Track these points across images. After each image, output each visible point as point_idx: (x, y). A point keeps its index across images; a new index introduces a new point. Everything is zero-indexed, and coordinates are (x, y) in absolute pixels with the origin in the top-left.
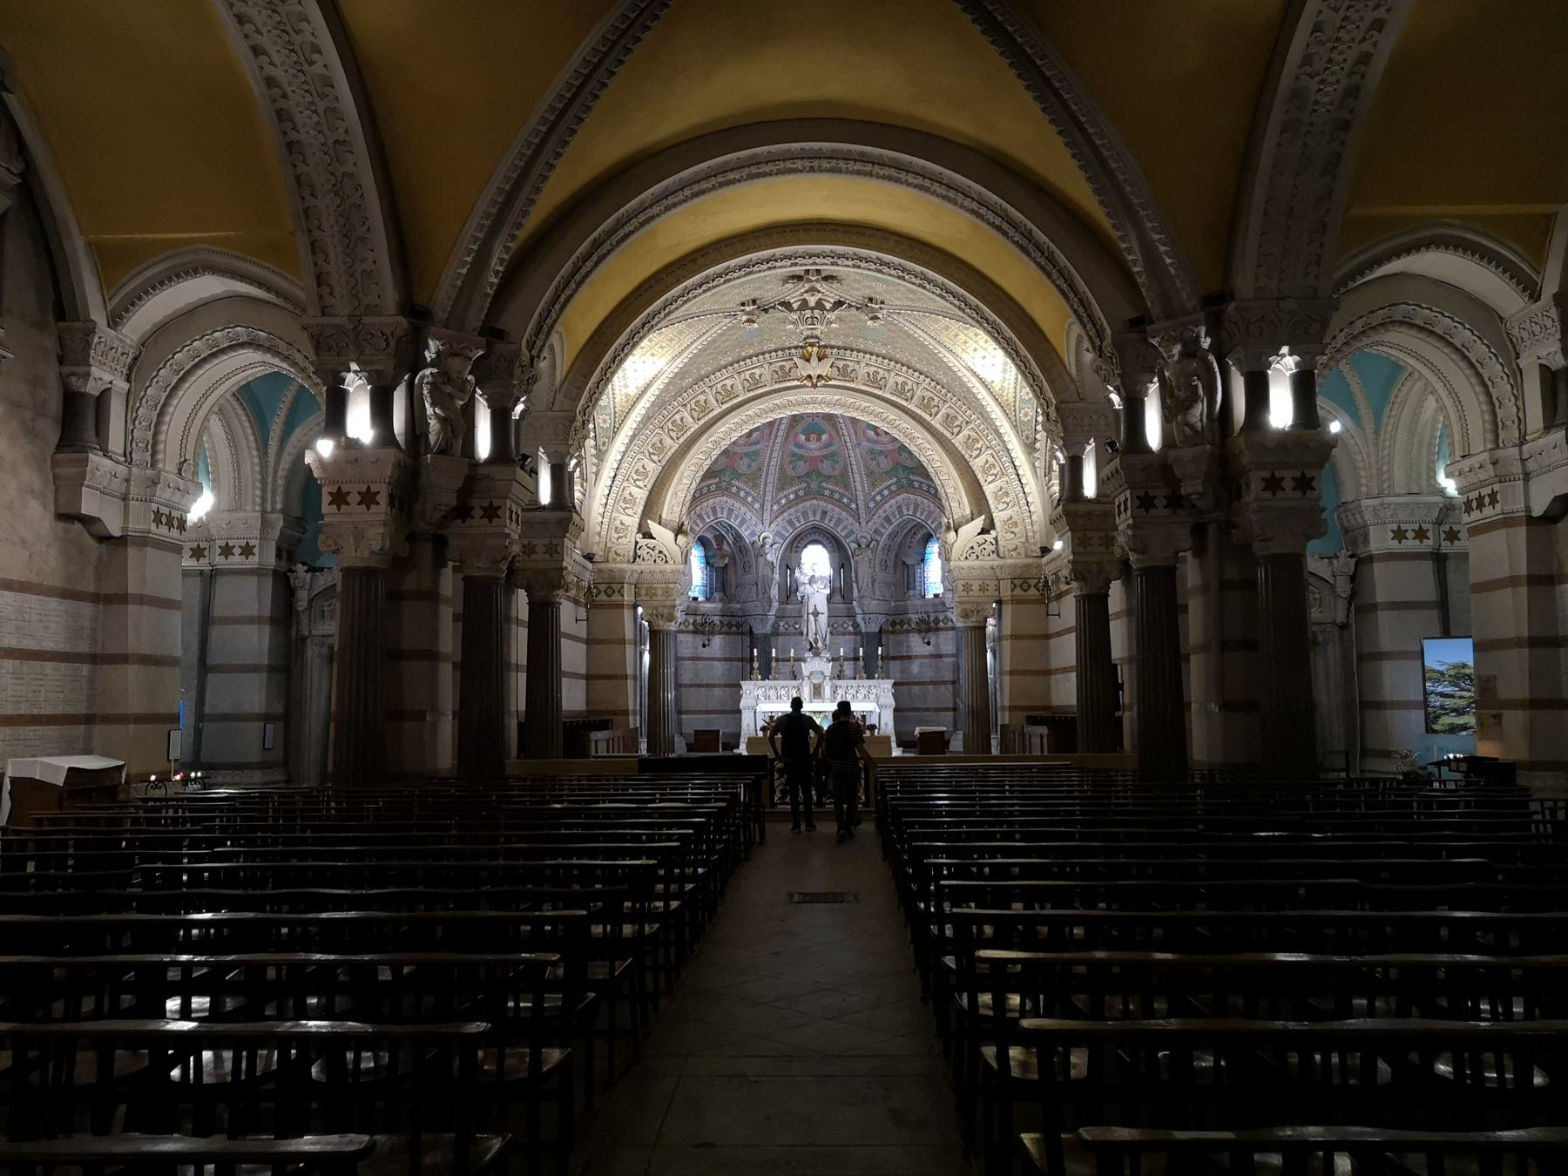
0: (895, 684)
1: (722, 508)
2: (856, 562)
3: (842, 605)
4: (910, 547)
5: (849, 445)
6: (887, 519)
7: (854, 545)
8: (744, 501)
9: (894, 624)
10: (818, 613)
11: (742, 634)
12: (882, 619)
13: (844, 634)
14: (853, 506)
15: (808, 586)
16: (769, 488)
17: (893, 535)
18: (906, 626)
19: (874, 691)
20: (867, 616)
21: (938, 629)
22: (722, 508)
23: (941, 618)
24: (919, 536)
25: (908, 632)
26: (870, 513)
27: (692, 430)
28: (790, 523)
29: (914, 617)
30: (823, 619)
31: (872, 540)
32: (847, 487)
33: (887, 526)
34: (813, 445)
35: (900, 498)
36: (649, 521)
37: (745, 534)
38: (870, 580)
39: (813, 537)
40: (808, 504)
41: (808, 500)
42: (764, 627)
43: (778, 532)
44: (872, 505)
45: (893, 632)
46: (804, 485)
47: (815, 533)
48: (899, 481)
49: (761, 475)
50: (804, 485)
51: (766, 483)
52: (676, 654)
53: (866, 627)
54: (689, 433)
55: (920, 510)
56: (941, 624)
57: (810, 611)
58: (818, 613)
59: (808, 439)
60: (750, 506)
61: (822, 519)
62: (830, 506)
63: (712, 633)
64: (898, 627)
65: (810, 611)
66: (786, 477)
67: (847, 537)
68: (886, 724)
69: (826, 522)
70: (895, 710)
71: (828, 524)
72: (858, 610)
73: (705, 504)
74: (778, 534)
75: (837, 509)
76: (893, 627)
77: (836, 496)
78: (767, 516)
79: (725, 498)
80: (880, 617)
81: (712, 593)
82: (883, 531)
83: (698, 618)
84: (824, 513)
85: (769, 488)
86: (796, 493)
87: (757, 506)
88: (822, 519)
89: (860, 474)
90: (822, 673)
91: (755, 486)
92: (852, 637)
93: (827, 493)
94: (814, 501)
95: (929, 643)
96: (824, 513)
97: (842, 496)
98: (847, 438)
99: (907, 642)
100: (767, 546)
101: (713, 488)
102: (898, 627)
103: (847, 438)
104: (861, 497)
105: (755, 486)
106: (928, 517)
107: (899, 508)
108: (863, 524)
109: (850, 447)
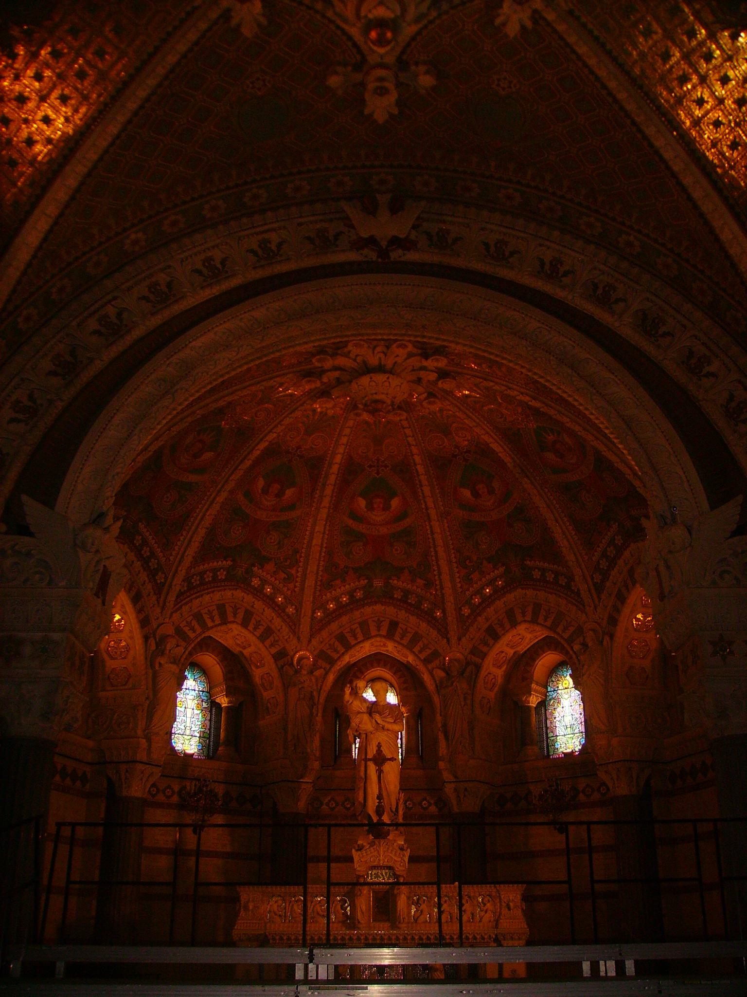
0: (525, 898)
5: (432, 512)
8: (270, 601)
15: (366, 717)
16: (310, 582)
27: (138, 333)
30: (392, 772)
34: (378, 517)
36: (25, 498)
40: (368, 610)
43: (322, 651)
44: (466, 611)
54: (129, 339)
56: (582, 797)
57: (370, 756)
59: (370, 507)
60: (280, 610)
62: (402, 614)
65: (370, 756)
72: (446, 776)
73: (207, 598)
75: (413, 619)
77: (412, 600)
78: (305, 627)
79: (239, 594)
81: (216, 750)
85: (310, 582)
87: (291, 610)
93: (398, 595)
94: (379, 607)
98: (430, 504)
100: (304, 672)
101: (222, 575)
103: (430, 504)
108: (454, 640)
109: (434, 516)
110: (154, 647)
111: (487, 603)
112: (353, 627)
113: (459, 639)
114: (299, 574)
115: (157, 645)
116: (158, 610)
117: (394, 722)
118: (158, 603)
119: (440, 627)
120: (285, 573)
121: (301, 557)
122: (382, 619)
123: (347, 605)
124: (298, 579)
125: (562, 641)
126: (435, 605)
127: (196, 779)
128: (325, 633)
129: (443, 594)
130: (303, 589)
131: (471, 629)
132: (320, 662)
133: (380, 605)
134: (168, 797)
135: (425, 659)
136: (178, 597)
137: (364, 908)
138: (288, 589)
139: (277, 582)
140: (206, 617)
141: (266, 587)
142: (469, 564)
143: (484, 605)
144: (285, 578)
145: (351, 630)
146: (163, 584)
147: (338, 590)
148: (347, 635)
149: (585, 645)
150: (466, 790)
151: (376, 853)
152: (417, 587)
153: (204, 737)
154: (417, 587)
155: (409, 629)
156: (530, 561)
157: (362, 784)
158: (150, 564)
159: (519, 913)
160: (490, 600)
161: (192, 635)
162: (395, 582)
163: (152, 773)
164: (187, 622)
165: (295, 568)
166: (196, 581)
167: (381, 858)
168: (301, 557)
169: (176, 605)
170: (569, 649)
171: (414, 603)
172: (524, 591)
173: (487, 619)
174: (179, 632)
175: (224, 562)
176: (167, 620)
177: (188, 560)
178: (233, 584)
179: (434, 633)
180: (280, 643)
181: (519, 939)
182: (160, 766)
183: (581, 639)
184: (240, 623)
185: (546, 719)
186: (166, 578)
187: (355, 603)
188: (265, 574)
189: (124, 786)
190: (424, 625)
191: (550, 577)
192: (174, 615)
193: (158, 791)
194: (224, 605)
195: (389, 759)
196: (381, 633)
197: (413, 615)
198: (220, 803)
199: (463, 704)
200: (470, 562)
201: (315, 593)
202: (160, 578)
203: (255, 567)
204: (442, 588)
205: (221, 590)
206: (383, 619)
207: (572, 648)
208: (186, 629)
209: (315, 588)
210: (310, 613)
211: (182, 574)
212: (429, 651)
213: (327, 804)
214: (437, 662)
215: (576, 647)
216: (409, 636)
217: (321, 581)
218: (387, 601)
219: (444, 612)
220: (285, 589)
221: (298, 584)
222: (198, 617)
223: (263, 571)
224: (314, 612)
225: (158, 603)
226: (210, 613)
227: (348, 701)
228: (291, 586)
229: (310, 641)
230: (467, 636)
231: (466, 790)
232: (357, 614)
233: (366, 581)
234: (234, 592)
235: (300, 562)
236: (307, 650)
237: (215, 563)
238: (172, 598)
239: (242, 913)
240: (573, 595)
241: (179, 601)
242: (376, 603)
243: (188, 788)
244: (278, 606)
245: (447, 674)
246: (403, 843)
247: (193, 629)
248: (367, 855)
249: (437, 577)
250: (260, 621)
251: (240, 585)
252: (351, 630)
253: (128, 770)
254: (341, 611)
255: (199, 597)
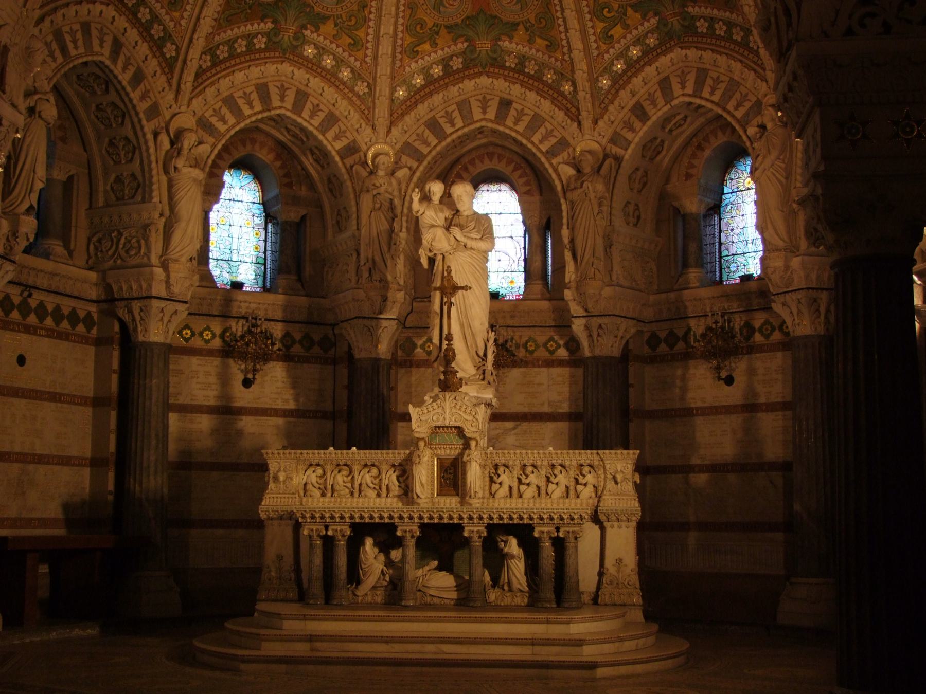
0: (641, 468)
1: (283, 90)
2: (572, 204)
3: (545, 305)
4: (688, 176)
6: (640, 112)
7: (568, 171)
8: (331, 77)
9: (654, 340)
10: (456, 288)
11: (334, 362)
12: (626, 329)
13: (549, 364)
14: (567, 88)
15: (440, 232)
16: (386, 47)
17: (651, 148)
18: (681, 346)
19: (590, 478)
20: (596, 322)
21: (751, 350)
22: (283, 90)
23: (757, 324)
24: (708, 153)
25: (687, 356)
26: (603, 103)
28: (433, 126)
29: (698, 327)
31: (606, 156)
32: (552, 46)
33: (637, 124)
35: (664, 60)
37: (333, 145)
38: (600, 242)
39: (487, 165)
41: (470, 77)
42: (376, 342)
43: (407, 145)
44: (605, 82)
45: (652, 360)
46: (462, 46)
47: (491, 156)
48: (663, 22)
49: (366, 20)
50: (462, 46)
51: (377, 38)
52: (166, 395)
53: (592, 345)
55: (709, 81)
56: (758, 338)
58: (456, 288)
61: (501, 116)
62: (516, 90)
63: (266, 358)
64: (663, 348)
66: (422, 24)
67: (551, 153)
68: (619, 561)
69: (510, 122)
70: (641, 527)
71: (514, 128)
72: (575, 309)
73: (239, 77)
74: (407, 149)
75: (532, 96)
76: (653, 347)
77: (531, 68)
78: (382, 112)
79: (286, 68)
80: (624, 324)
82: (629, 136)
83: (233, 323)
84: (505, 104)
85: (386, 47)
86: (445, 62)
87: (361, 88)
88: (501, 116)
89: (579, 13)
90: (460, 430)
91: (356, 45)
92: (565, 371)
93: (510, 62)
94: (484, 81)
95: (729, 381)
96: (505, 104)
97: (542, 66)
99: (684, 379)
100: (381, 173)
101: (260, 43)
102: (663, 348)
104: (581, 66)
105: (356, 45)
106: (727, 95)
107: (665, 84)
108: (587, 124)
110: (166, 144)
111: (633, 70)
112: (450, 109)
113: (596, 122)
114: (370, 38)
115: (172, 143)
116: (171, 96)
117: (481, 239)
118: (170, 85)
119: (569, 106)
120: (350, 37)
121: (370, 13)
122: (488, 97)
123: (441, 78)
124: (370, 45)
125: (734, 123)
126: (562, 74)
127: (243, 317)
128: (409, 119)
129: (571, 59)
130: (376, 58)
131: (611, 108)
132: (404, 159)
133: (486, 78)
134: (207, 342)
135: (547, 152)
136: (197, 76)
137: (424, 479)
138: (356, 60)
139: (340, 50)
140: (241, 102)
141: (325, 57)
142: (608, 15)
143: (629, 74)
144: (350, 44)
145: (447, 112)
146: (176, 59)
147: (427, 58)
148: (442, 121)
149: (763, 127)
150: (600, 327)
151: (440, 410)
152: (538, 51)
153: (258, 263)
154: (538, 51)
155: (526, 111)
156: (693, 7)
157: (437, 321)
158: (153, 32)
159: (629, 488)
160: (638, 66)
161: (222, 128)
162: (507, 43)
163: (176, 311)
164: (214, 110)
165: (363, 29)
166: (222, 52)
167: (447, 416)
168: (370, 13)
169: (198, 87)
170: (741, 133)
171: (533, 73)
172: (684, 52)
173: (633, 94)
174: (204, 125)
175: (262, 25)
176: (183, 109)
177: (206, 25)
178: (277, 54)
179: (560, 115)
180: (348, 134)
181: (628, 520)
182: (186, 302)
183: (758, 120)
184: (290, 109)
185: (720, 231)
186: (178, 50)
187: (450, 76)
188: (321, 38)
189: (139, 329)
190: (546, 105)
191: (720, 29)
192: (194, 101)
193: (193, 334)
194: (265, 85)
195: (462, 288)
196: (487, 116)
197: (530, 90)
198: (276, 347)
199: (596, 212)
200: (609, 12)
201: (393, 63)
202: (169, 50)
203: (306, 29)
204: (570, 51)
205: (260, 65)
206: (492, 97)
207: (745, 131)
208: (213, 120)
209: (394, 56)
210: (387, 91)
211: (200, 43)
212: (554, 141)
213: (422, 347)
214: (565, 155)
215: (752, 131)
216: (526, 119)
217: (402, 46)
218: (496, 71)
219: (574, 84)
220: (352, 59)
221: (369, 52)
222: (230, 102)
223: (319, 35)
224: (393, 90)
225: (170, 85)
226: (246, 96)
227: (418, 212)
228: (360, 54)
229: (389, 131)
230: (606, 117)
231: (600, 327)
232: (454, 91)
233: (466, 45)
234: (279, 66)
235: (370, 20)
236: (386, 143)
237: (249, 27)
238: (189, 77)
239: (272, 485)
240: (751, 56)
241: (200, 80)
242: (480, 74)
243: (234, 329)
244: (344, 84)
245: (579, 171)
246: (491, 396)
247: (223, 120)
248: (428, 412)
249: (563, 36)
250: (318, 105)
251: (287, 56)
252: (447, 112)
253: (143, 308)
254: (432, 88)
255: (228, 75)
